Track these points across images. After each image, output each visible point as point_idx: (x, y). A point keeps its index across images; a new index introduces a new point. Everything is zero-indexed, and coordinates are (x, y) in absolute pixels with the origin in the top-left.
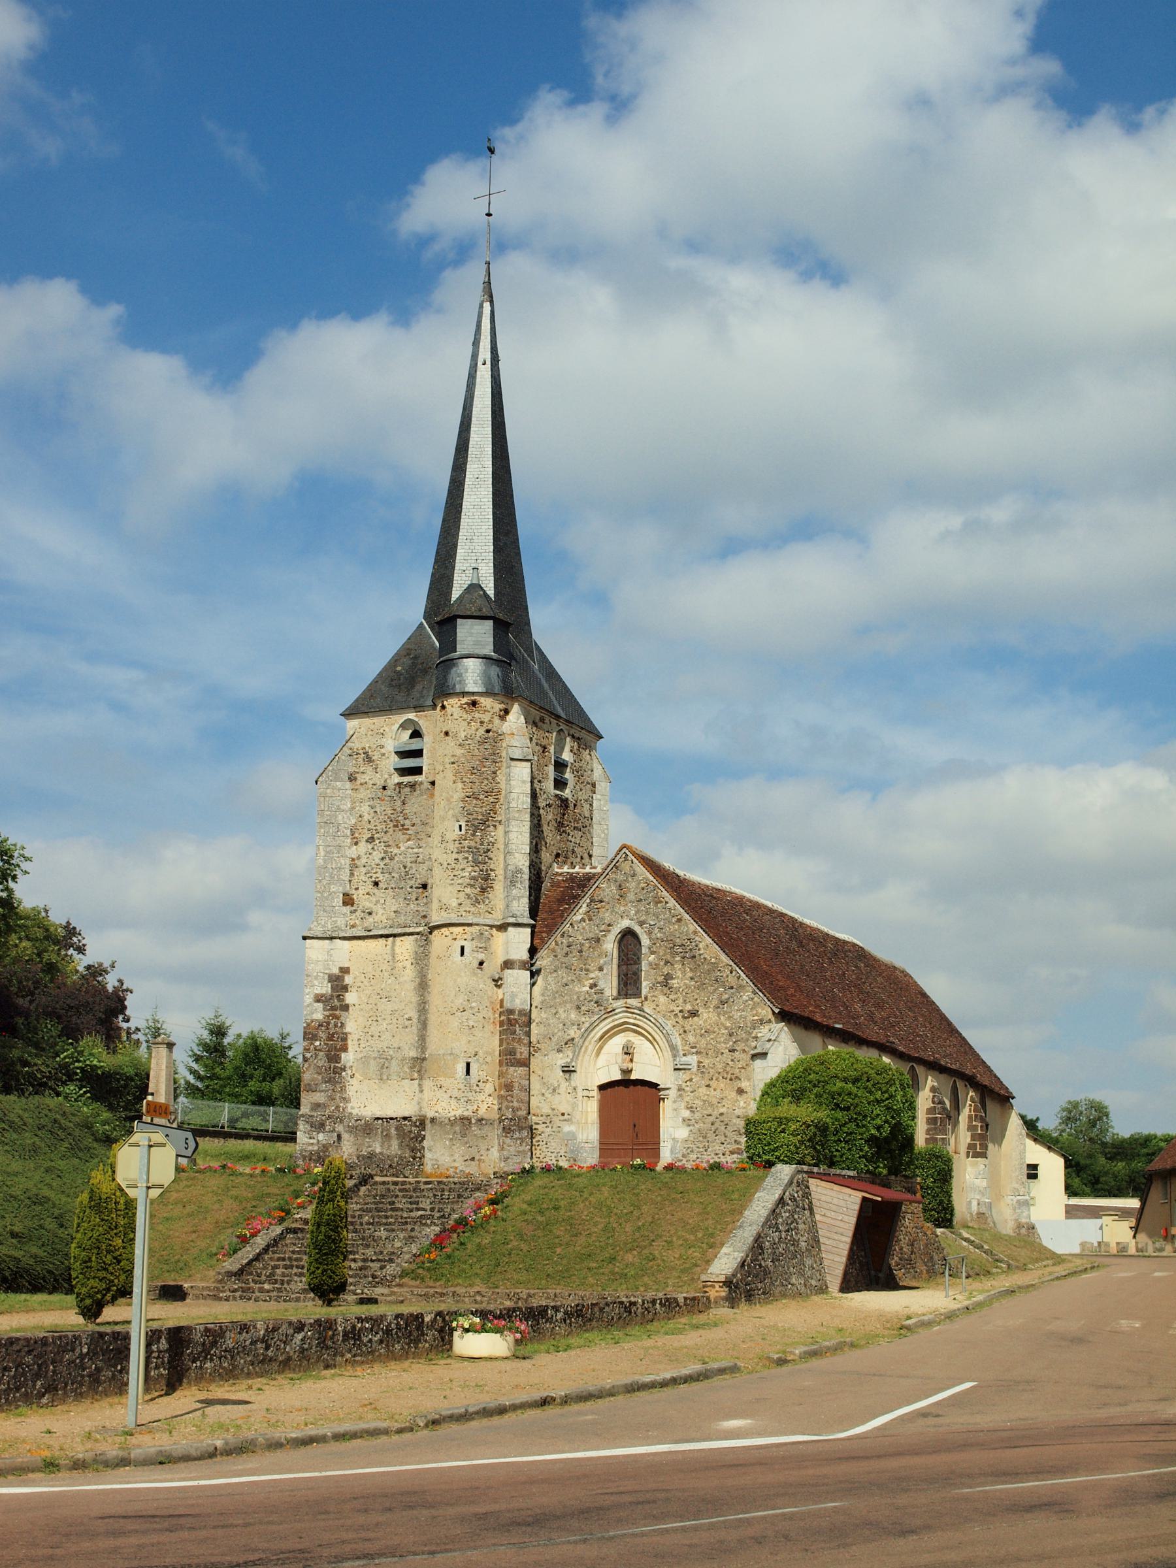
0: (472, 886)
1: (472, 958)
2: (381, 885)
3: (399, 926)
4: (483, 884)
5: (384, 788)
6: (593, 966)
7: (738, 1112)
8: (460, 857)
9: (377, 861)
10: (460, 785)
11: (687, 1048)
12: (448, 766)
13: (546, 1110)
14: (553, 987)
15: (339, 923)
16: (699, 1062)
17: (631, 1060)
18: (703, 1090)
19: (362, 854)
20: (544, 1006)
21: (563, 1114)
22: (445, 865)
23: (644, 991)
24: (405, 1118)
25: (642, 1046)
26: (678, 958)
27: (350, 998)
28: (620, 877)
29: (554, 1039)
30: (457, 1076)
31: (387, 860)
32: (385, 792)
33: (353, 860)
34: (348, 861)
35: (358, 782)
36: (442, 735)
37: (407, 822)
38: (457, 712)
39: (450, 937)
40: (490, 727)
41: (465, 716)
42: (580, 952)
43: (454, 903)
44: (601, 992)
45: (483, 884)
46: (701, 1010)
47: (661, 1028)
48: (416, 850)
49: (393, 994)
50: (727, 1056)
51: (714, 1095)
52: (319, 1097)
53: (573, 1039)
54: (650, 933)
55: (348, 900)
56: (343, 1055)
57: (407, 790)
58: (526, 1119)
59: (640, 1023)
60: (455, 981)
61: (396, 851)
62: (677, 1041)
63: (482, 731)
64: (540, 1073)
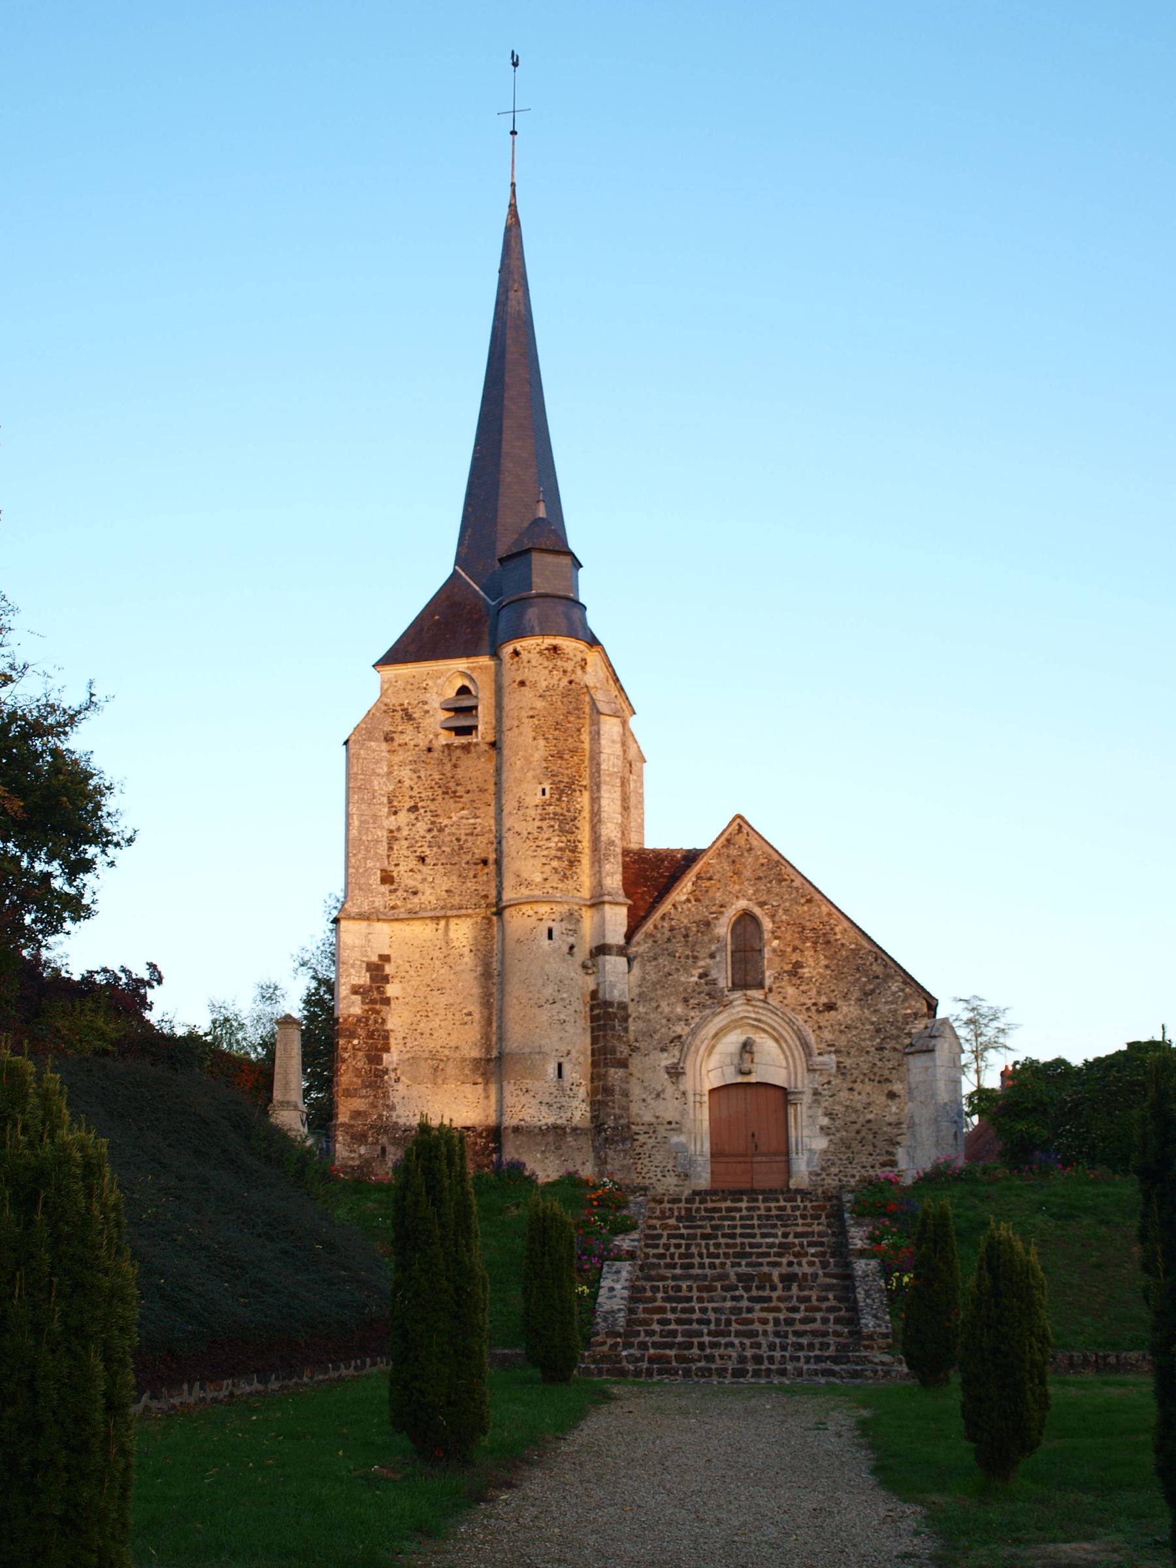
0: (560, 858)
1: (561, 943)
2: (428, 860)
3: (452, 907)
4: (570, 856)
5: (429, 750)
6: (703, 952)
7: (888, 1119)
8: (545, 824)
9: (422, 833)
10: (542, 742)
11: (823, 1046)
12: (526, 721)
13: (648, 1118)
14: (653, 977)
15: (377, 904)
16: (839, 1063)
17: (752, 1061)
18: (844, 1094)
19: (403, 825)
20: (642, 998)
21: (670, 1123)
22: (525, 834)
23: (768, 982)
24: (468, 1128)
25: (766, 1045)
26: (808, 944)
27: (391, 990)
28: (734, 852)
29: (657, 1037)
30: (548, 1078)
31: (435, 833)
32: (430, 755)
33: (391, 831)
34: (385, 834)
35: (396, 744)
36: (515, 685)
37: (459, 788)
38: (535, 659)
39: (534, 918)
40: (573, 677)
41: (546, 663)
42: (686, 936)
43: (538, 878)
44: (714, 982)
45: (570, 856)
46: (839, 1003)
47: (790, 1023)
48: (472, 821)
49: (448, 986)
50: (874, 1057)
51: (858, 1100)
52: (359, 1104)
53: (680, 1037)
54: (773, 916)
55: (387, 878)
56: (385, 1056)
57: (458, 752)
58: (629, 1127)
59: (763, 1018)
60: (542, 968)
61: (446, 822)
62: (812, 1039)
63: (565, 682)
64: (639, 1075)
